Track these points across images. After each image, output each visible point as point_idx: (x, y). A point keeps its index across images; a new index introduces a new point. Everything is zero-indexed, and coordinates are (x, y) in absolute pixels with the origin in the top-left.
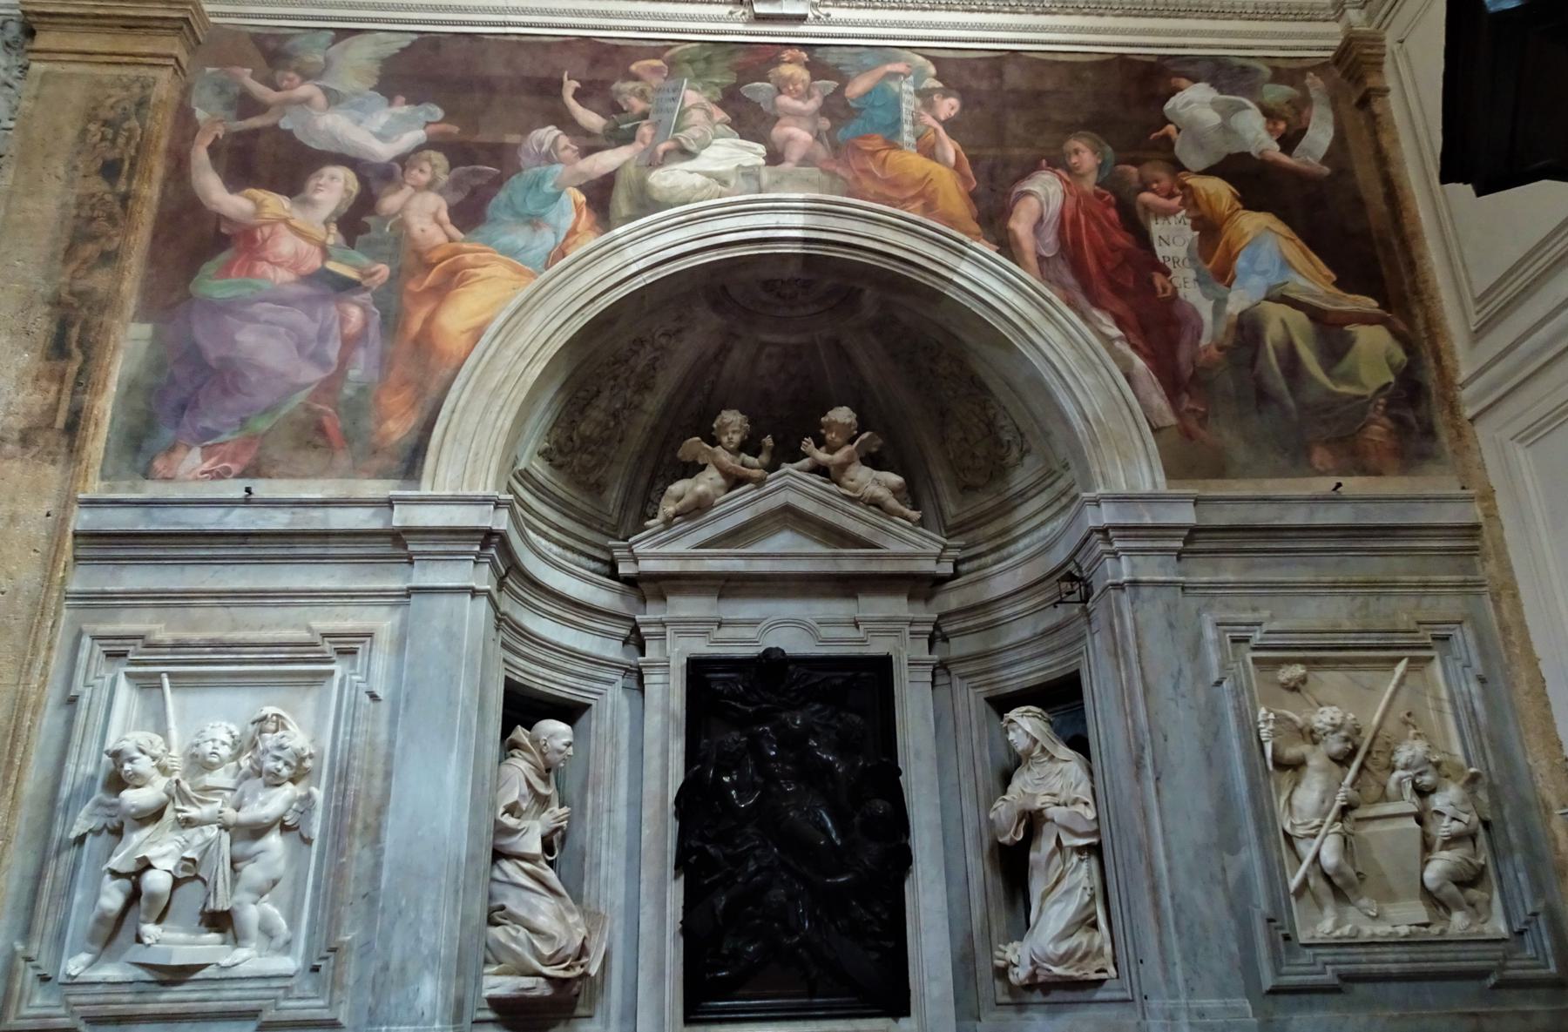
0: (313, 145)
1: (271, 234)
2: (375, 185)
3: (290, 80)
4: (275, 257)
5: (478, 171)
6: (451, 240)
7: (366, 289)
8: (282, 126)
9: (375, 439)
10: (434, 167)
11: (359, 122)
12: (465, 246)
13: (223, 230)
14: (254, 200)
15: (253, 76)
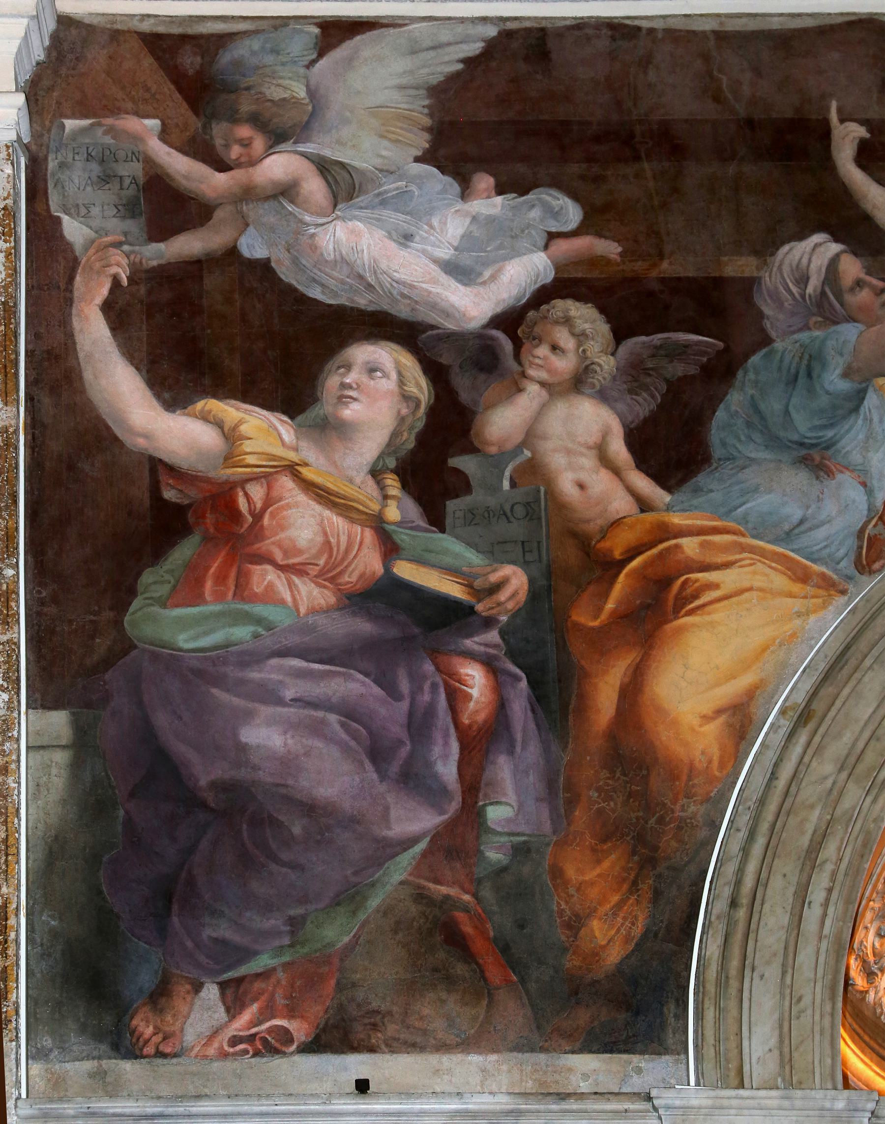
0: (316, 293)
1: (268, 502)
2: (462, 383)
3: (246, 144)
4: (286, 553)
5: (677, 344)
6: (644, 505)
7: (488, 623)
8: (246, 252)
9: (570, 962)
10: (581, 337)
11: (406, 239)
12: (677, 519)
13: (169, 494)
14: (219, 424)
15: (164, 135)
